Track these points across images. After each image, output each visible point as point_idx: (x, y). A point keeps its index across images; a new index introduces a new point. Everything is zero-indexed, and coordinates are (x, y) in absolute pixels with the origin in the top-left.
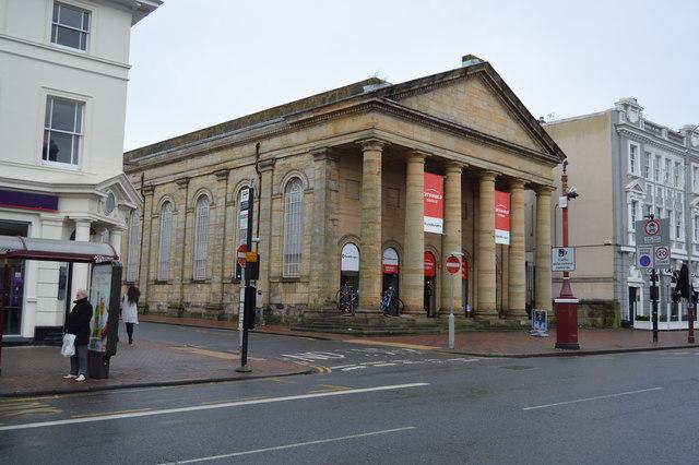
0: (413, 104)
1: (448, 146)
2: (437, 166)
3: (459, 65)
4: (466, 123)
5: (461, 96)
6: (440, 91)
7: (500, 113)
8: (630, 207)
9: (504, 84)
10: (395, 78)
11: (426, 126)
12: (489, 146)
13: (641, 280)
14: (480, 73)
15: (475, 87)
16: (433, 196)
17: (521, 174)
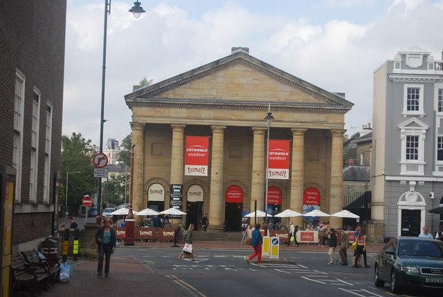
0: (170, 95)
1: (205, 117)
2: (197, 132)
3: (229, 53)
4: (226, 97)
5: (220, 80)
6: (198, 81)
7: (270, 82)
8: (404, 143)
9: (263, 63)
10: (155, 78)
11: (181, 107)
12: (252, 110)
13: (423, 203)
14: (239, 58)
15: (239, 69)
16: (198, 150)
17: (298, 125)
